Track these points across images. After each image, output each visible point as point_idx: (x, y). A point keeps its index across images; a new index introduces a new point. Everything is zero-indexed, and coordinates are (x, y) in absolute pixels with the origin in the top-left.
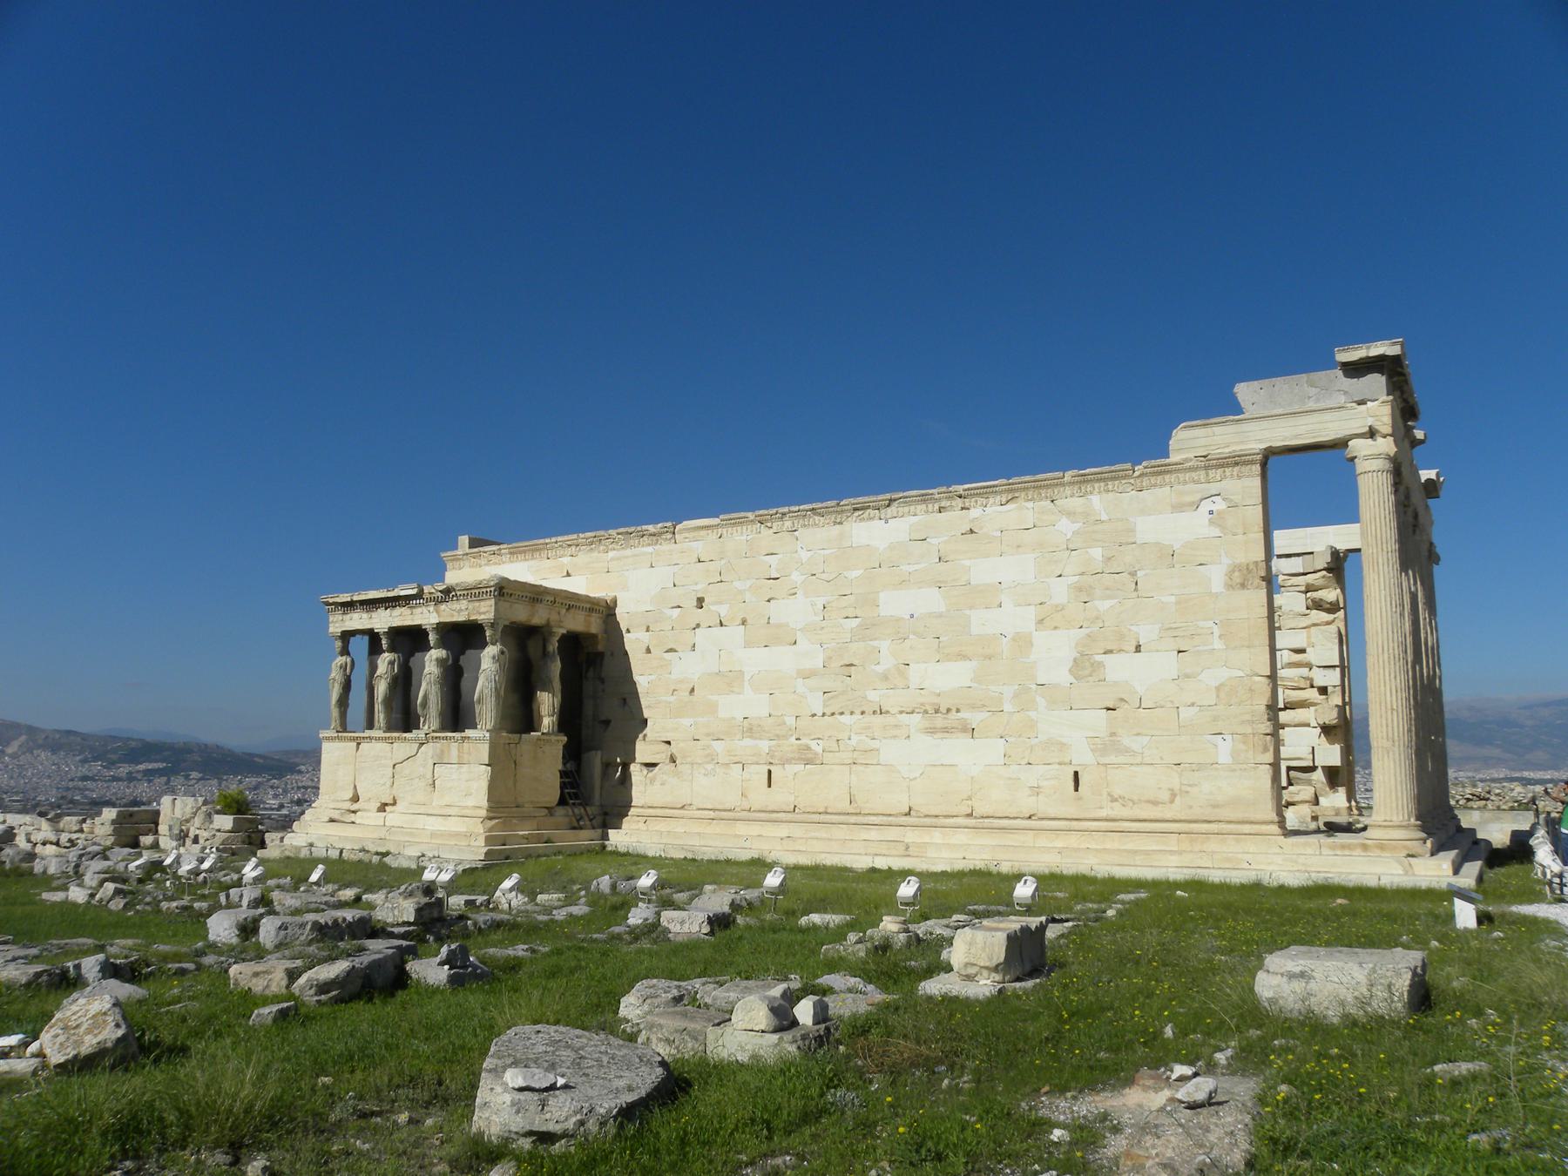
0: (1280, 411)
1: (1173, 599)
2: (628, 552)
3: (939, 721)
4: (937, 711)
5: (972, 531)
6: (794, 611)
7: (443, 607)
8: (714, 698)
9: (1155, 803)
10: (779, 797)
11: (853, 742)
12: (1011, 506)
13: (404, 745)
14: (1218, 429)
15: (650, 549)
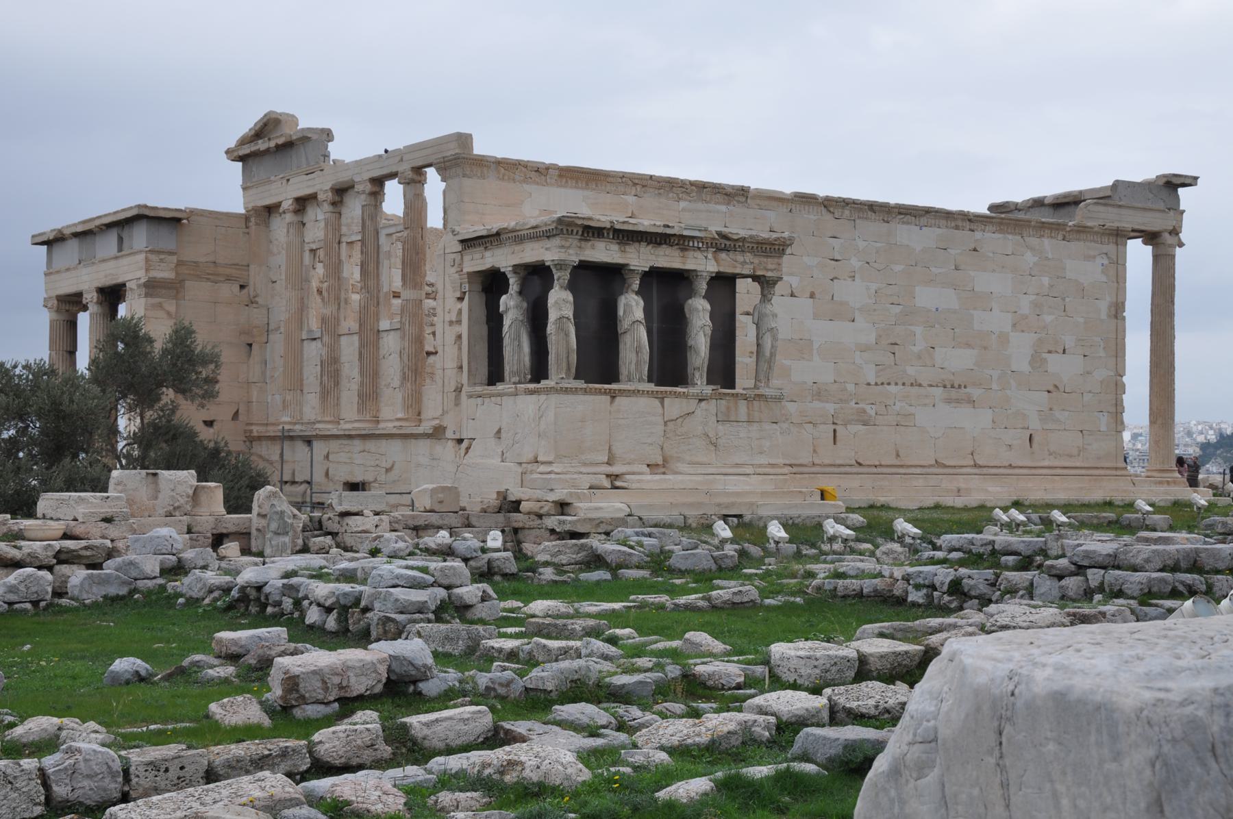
0: (1140, 205)
1: (1082, 320)
2: (701, 206)
3: (954, 394)
4: (953, 387)
5: (975, 250)
6: (854, 293)
7: (723, 255)
8: (787, 362)
9: (1071, 456)
10: (844, 454)
11: (897, 407)
12: (997, 235)
13: (676, 403)
14: (1110, 209)
15: (723, 208)
